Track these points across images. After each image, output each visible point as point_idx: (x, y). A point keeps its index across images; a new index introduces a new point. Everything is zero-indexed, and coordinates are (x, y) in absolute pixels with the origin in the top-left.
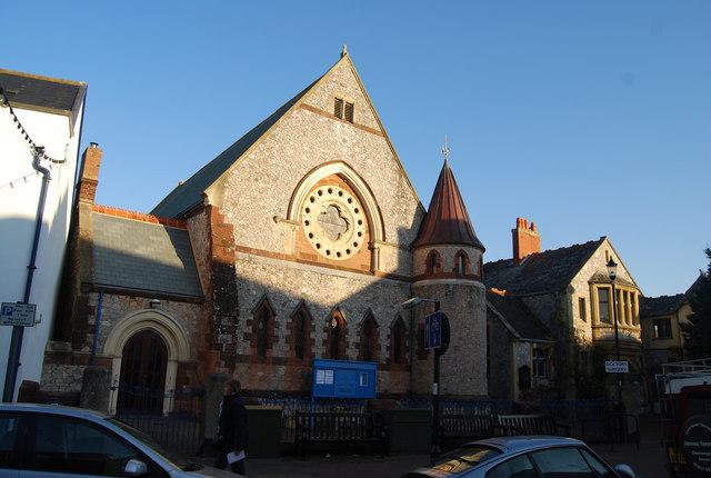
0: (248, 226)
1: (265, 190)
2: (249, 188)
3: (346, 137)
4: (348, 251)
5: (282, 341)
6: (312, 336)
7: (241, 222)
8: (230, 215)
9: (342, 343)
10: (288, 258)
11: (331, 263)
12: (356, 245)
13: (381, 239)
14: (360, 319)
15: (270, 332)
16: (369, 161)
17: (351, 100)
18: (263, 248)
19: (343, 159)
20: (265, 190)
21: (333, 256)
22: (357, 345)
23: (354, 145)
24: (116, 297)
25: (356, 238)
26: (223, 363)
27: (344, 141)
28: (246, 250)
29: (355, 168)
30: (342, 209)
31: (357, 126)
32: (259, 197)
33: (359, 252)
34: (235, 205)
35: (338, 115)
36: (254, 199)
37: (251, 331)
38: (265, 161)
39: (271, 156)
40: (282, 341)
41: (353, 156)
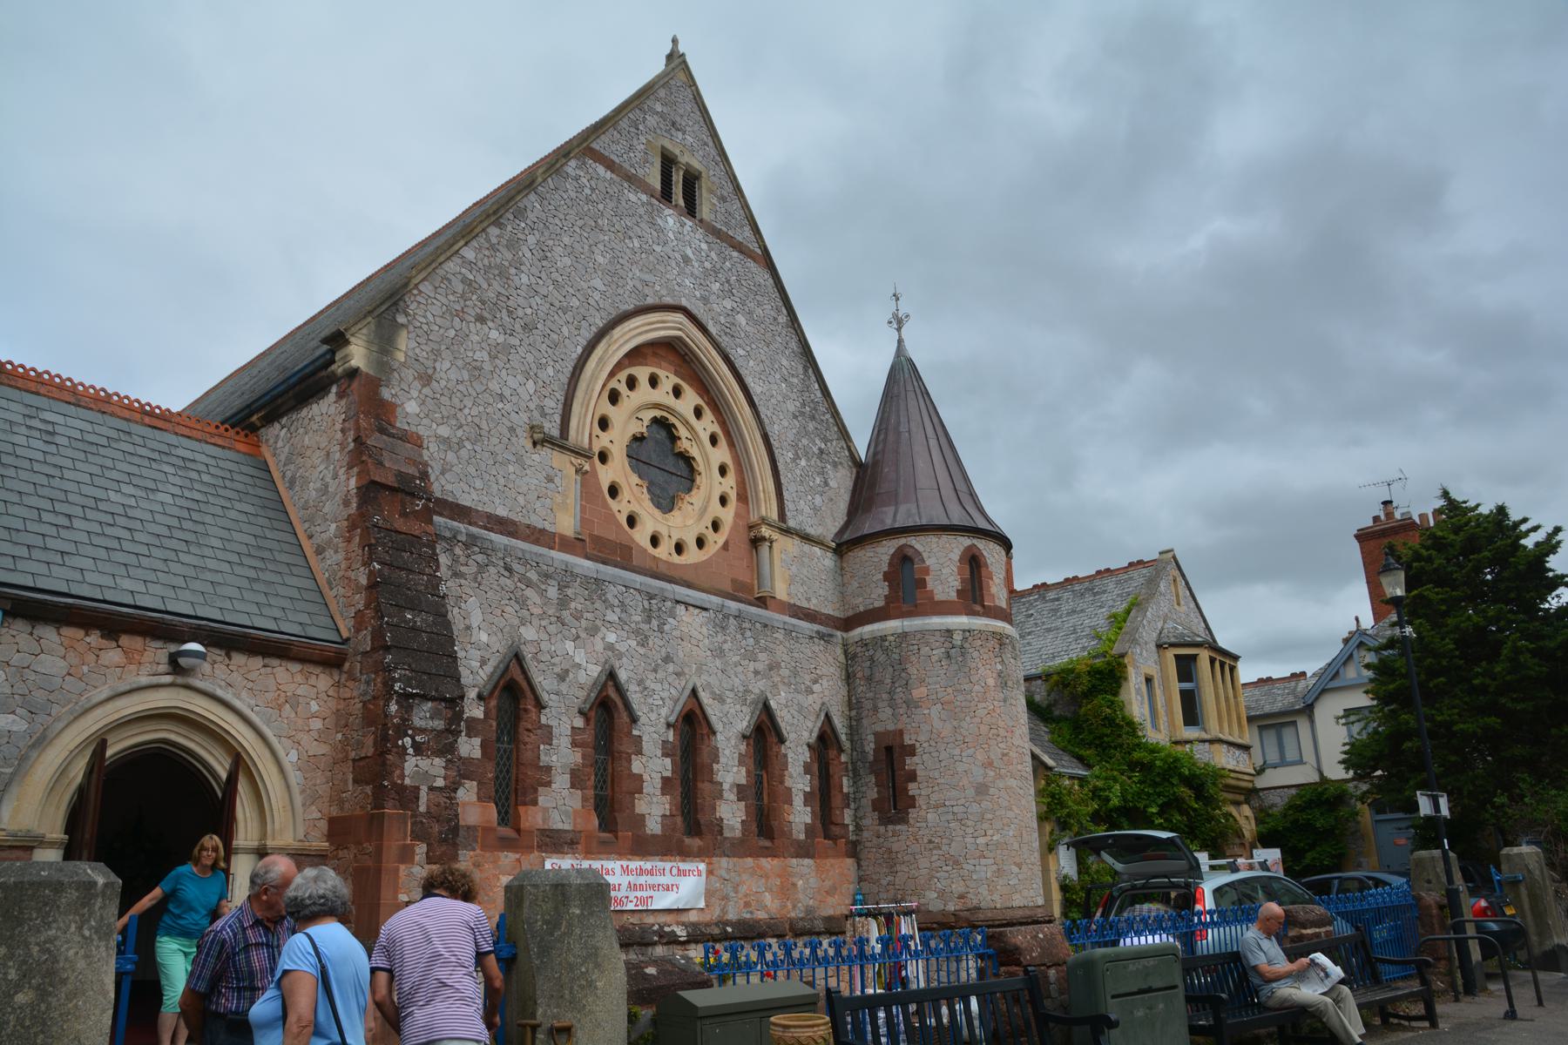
0: (460, 445)
1: (507, 349)
2: (462, 337)
5: (561, 781)
6: (637, 766)
7: (444, 431)
8: (412, 407)
10: (567, 545)
11: (663, 569)
15: (527, 755)
17: (696, 164)
18: (501, 512)
19: (684, 302)
20: (507, 349)
21: (664, 551)
24: (48, 633)
25: (715, 509)
26: (421, 849)
28: (460, 512)
29: (713, 330)
32: (487, 367)
33: (726, 546)
34: (426, 379)
36: (476, 370)
38: (503, 274)
40: (561, 781)
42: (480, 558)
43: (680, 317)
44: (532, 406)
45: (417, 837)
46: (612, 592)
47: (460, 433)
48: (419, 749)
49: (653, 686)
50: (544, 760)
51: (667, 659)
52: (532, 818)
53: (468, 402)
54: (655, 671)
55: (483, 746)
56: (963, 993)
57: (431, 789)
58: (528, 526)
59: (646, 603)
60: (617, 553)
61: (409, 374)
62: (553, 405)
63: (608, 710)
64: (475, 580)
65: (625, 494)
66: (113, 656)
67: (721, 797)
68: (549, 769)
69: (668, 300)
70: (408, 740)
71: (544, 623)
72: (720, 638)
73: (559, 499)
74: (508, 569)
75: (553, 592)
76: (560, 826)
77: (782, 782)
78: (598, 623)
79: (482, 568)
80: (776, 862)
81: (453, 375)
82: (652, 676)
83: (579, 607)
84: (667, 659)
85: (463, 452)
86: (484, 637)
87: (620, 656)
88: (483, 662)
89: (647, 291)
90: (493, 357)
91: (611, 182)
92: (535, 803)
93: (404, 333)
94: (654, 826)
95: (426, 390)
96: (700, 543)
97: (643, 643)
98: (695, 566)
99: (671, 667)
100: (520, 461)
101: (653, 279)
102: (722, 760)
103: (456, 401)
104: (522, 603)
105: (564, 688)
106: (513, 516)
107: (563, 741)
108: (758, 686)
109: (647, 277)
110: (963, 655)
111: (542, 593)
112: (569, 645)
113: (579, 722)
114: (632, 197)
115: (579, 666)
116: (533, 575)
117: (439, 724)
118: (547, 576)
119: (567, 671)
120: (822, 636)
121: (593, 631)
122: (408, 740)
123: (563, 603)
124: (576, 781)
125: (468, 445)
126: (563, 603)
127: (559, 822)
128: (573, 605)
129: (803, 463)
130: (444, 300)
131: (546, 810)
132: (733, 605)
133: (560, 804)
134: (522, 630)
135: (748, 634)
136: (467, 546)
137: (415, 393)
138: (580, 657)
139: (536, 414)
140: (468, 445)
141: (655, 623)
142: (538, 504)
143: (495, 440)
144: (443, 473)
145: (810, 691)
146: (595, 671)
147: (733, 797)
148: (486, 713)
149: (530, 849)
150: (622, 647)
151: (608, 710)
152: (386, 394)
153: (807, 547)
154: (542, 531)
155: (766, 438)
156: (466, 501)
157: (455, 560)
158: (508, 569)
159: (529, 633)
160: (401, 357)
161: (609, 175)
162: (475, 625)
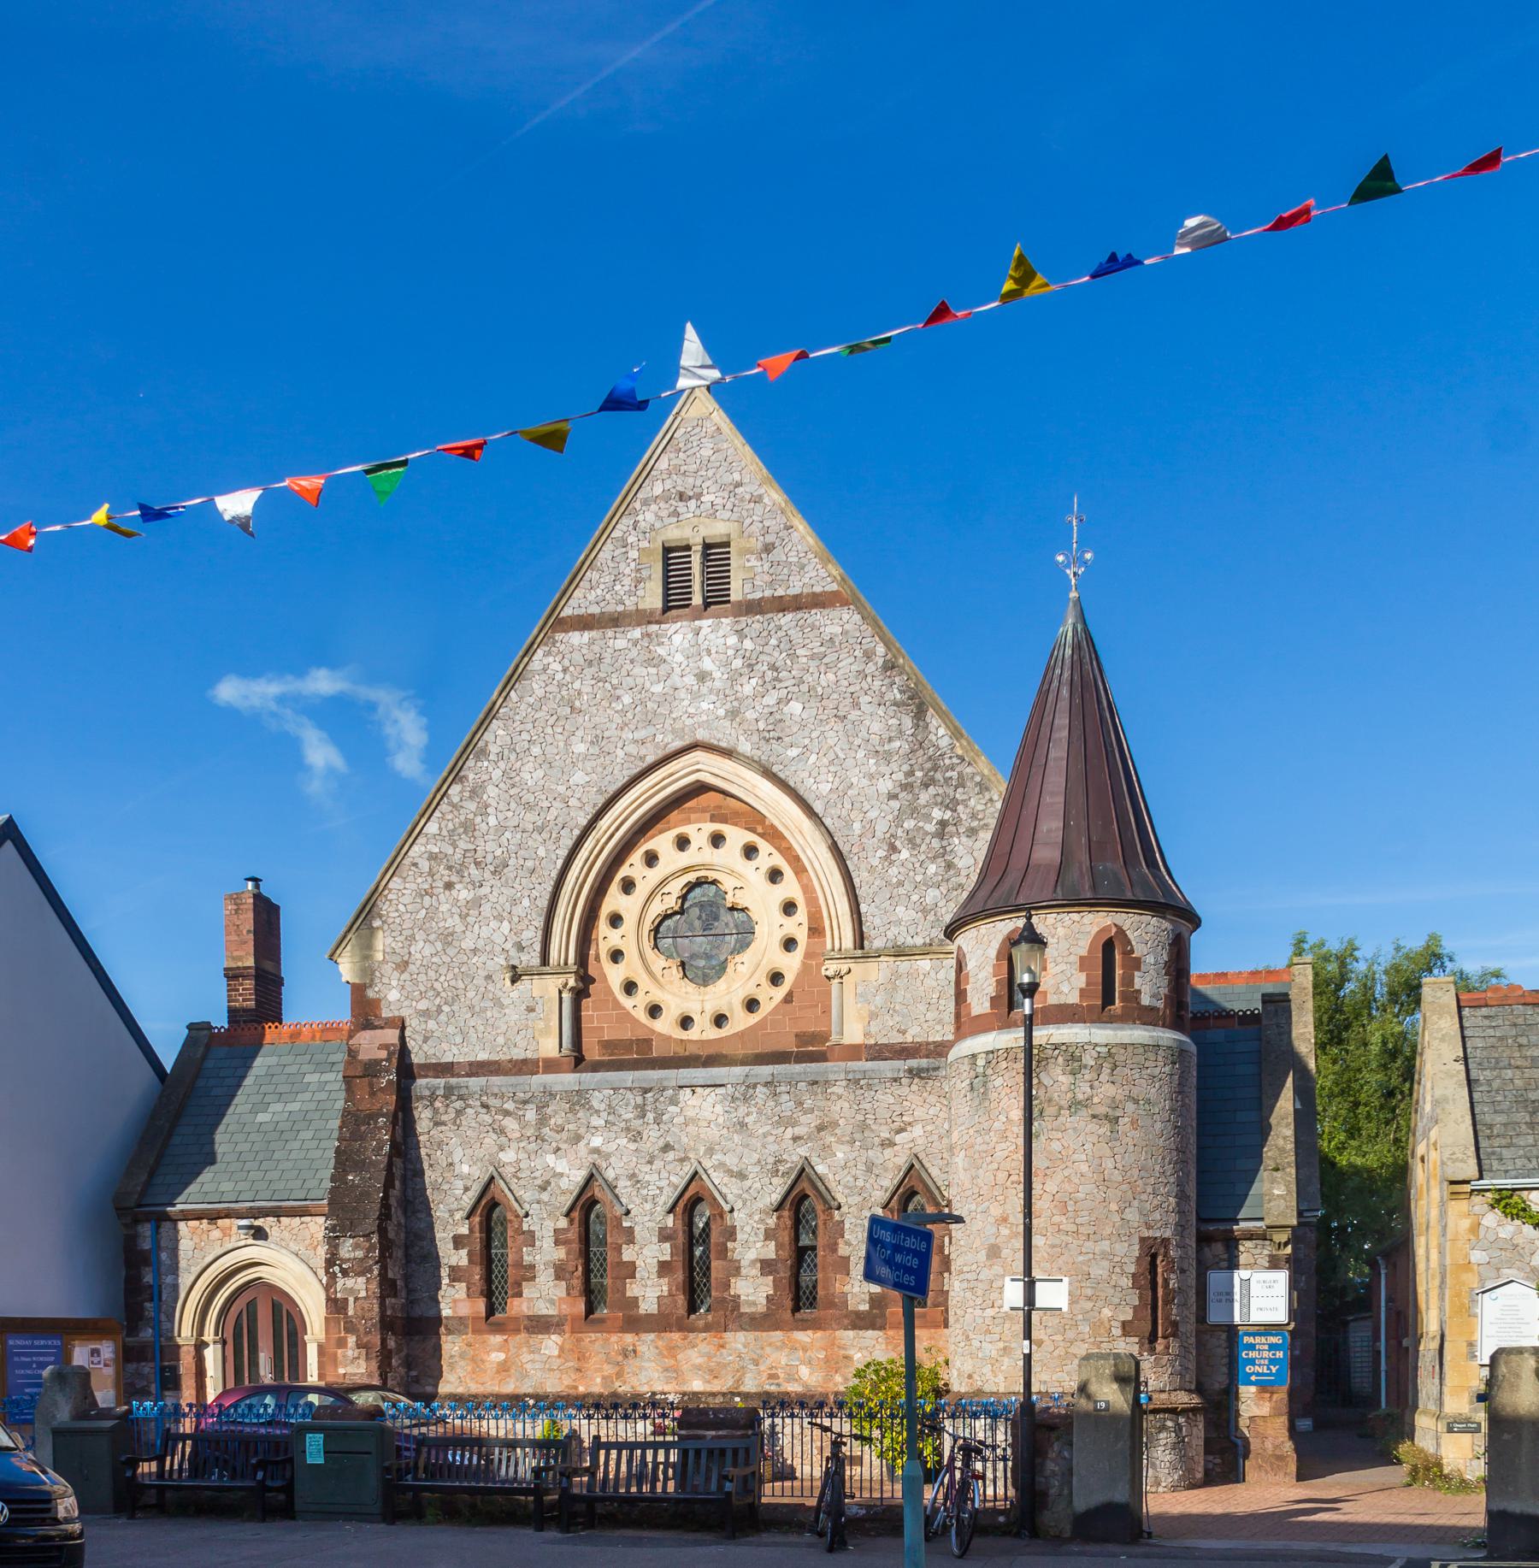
0: (439, 1011)
1: (477, 903)
2: (432, 912)
3: (707, 664)
4: (752, 1005)
5: (545, 1277)
6: (628, 1254)
7: (423, 1005)
8: (393, 995)
9: (715, 1264)
10: (551, 1066)
11: (692, 1050)
13: (848, 942)
14: (775, 1191)
16: (795, 707)
17: (716, 530)
18: (483, 1056)
19: (702, 735)
20: (477, 903)
21: (703, 1031)
22: (766, 1266)
23: (734, 678)
26: (352, 1340)
27: (702, 677)
28: (445, 1069)
29: (745, 747)
30: (657, 908)
31: (752, 608)
32: (460, 928)
33: (788, 999)
34: (403, 966)
35: (674, 601)
36: (448, 938)
37: (464, 1262)
38: (469, 827)
39: (483, 810)
40: (545, 1277)
41: (733, 714)
42: (459, 1104)
43: (698, 755)
44: (508, 946)
45: (347, 1330)
46: (596, 1100)
47: (437, 1001)
48: (345, 1273)
49: (647, 1177)
50: (527, 1259)
51: (667, 1148)
52: (518, 1307)
53: (443, 970)
54: (650, 1162)
55: (470, 1254)
56: (667, 1446)
57: (356, 1299)
58: (510, 1061)
59: (639, 1100)
61: (388, 968)
62: (532, 936)
63: (589, 1211)
64: (454, 1123)
65: (778, 936)
66: (216, 1234)
67: (737, 1271)
68: (532, 1267)
69: (678, 744)
70: (337, 1269)
71: (522, 1145)
72: (743, 1110)
73: (541, 1025)
74: (485, 1106)
75: (531, 1114)
76: (544, 1312)
77: (833, 1248)
78: (582, 1131)
79: (459, 1113)
80: (819, 1334)
81: (428, 951)
82: (647, 1168)
83: (560, 1122)
84: (667, 1148)
85: (443, 1017)
86: (465, 1169)
87: (607, 1156)
88: (466, 1189)
89: (643, 752)
90: (463, 917)
91: (592, 642)
92: (520, 1295)
93: (380, 934)
94: (648, 1306)
95: (405, 976)
96: (686, 1022)
97: (637, 1137)
98: (741, 1035)
99: (671, 1156)
100: (498, 1003)
101: (651, 730)
102: (739, 1236)
103: (431, 974)
104: (502, 1132)
105: (545, 1196)
106: (494, 1057)
107: (546, 1242)
108: (795, 1156)
109: (641, 734)
110: (985, 1084)
111: (520, 1119)
112: (550, 1159)
113: (563, 1223)
114: (621, 643)
115: (561, 1175)
116: (510, 1106)
117: (360, 1254)
118: (525, 1102)
119: (548, 1183)
120: (914, 1073)
121: (577, 1138)
122: (337, 1269)
123: (542, 1121)
124: (560, 1272)
125: (446, 1008)
126: (542, 1121)
127: (544, 1309)
128: (553, 1121)
129: (905, 854)
130: (414, 886)
131: (531, 1299)
132: (765, 1071)
133: (545, 1293)
134: (501, 1155)
135: (785, 1097)
136: (446, 1097)
137: (394, 983)
138: (561, 1166)
139: (513, 952)
140: (446, 1008)
141: (650, 1116)
142: (519, 1038)
143: (471, 994)
144: (425, 1042)
145: (888, 1143)
146: (579, 1176)
147: (756, 1271)
148: (471, 1230)
149: (517, 1331)
150: (612, 1147)
151: (589, 1211)
152: (371, 994)
153: (904, 965)
154: (525, 1061)
155: (835, 849)
156: (448, 1059)
157: (436, 1111)
158: (485, 1106)
159: (508, 1156)
160: (379, 956)
161: (587, 635)
162: (456, 1160)
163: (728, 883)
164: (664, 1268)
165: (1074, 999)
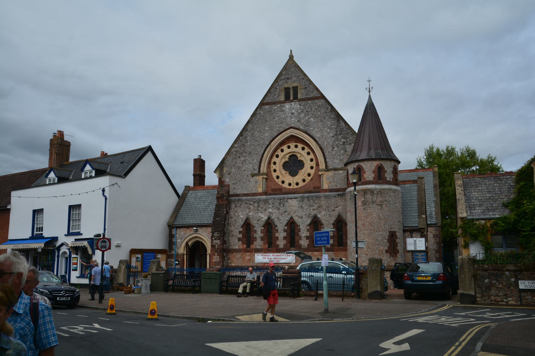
0: (237, 183)
1: (245, 160)
2: (236, 162)
3: (293, 111)
4: (304, 181)
6: (277, 235)
7: (233, 182)
8: (227, 180)
9: (296, 237)
10: (260, 194)
12: (309, 175)
13: (324, 167)
14: (309, 221)
15: (252, 236)
16: (312, 119)
17: (295, 85)
18: (246, 192)
19: (292, 125)
20: (245, 160)
22: (307, 238)
23: (299, 114)
24: (181, 229)
26: (216, 254)
27: (292, 114)
29: (302, 127)
31: (302, 100)
33: (312, 179)
34: (229, 174)
35: (287, 99)
36: (239, 168)
37: (241, 237)
38: (244, 145)
39: (247, 142)
41: (299, 121)
43: (291, 130)
48: (215, 239)
50: (255, 236)
52: (253, 247)
60: (279, 191)
61: (226, 174)
62: (256, 167)
66: (189, 231)
67: (301, 239)
68: (256, 238)
69: (287, 127)
74: (246, 203)
75: (256, 205)
79: (241, 204)
84: (285, 212)
86: (242, 216)
87: (272, 214)
90: (242, 163)
91: (270, 107)
97: (279, 209)
99: (286, 213)
100: (249, 181)
104: (250, 209)
105: (259, 222)
109: (280, 125)
112: (260, 214)
114: (275, 108)
116: (252, 203)
117: (219, 235)
120: (339, 195)
121: (266, 210)
123: (258, 206)
124: (262, 239)
126: (258, 206)
127: (258, 247)
129: (336, 149)
132: (307, 195)
133: (258, 243)
138: (262, 216)
141: (282, 205)
146: (266, 218)
147: (305, 239)
150: (273, 212)
151: (269, 225)
152: (223, 180)
153: (336, 172)
154: (255, 193)
156: (238, 193)
157: (236, 204)
158: (246, 203)
159: (251, 214)
163: (298, 155)
164: (285, 238)
165: (372, 179)
